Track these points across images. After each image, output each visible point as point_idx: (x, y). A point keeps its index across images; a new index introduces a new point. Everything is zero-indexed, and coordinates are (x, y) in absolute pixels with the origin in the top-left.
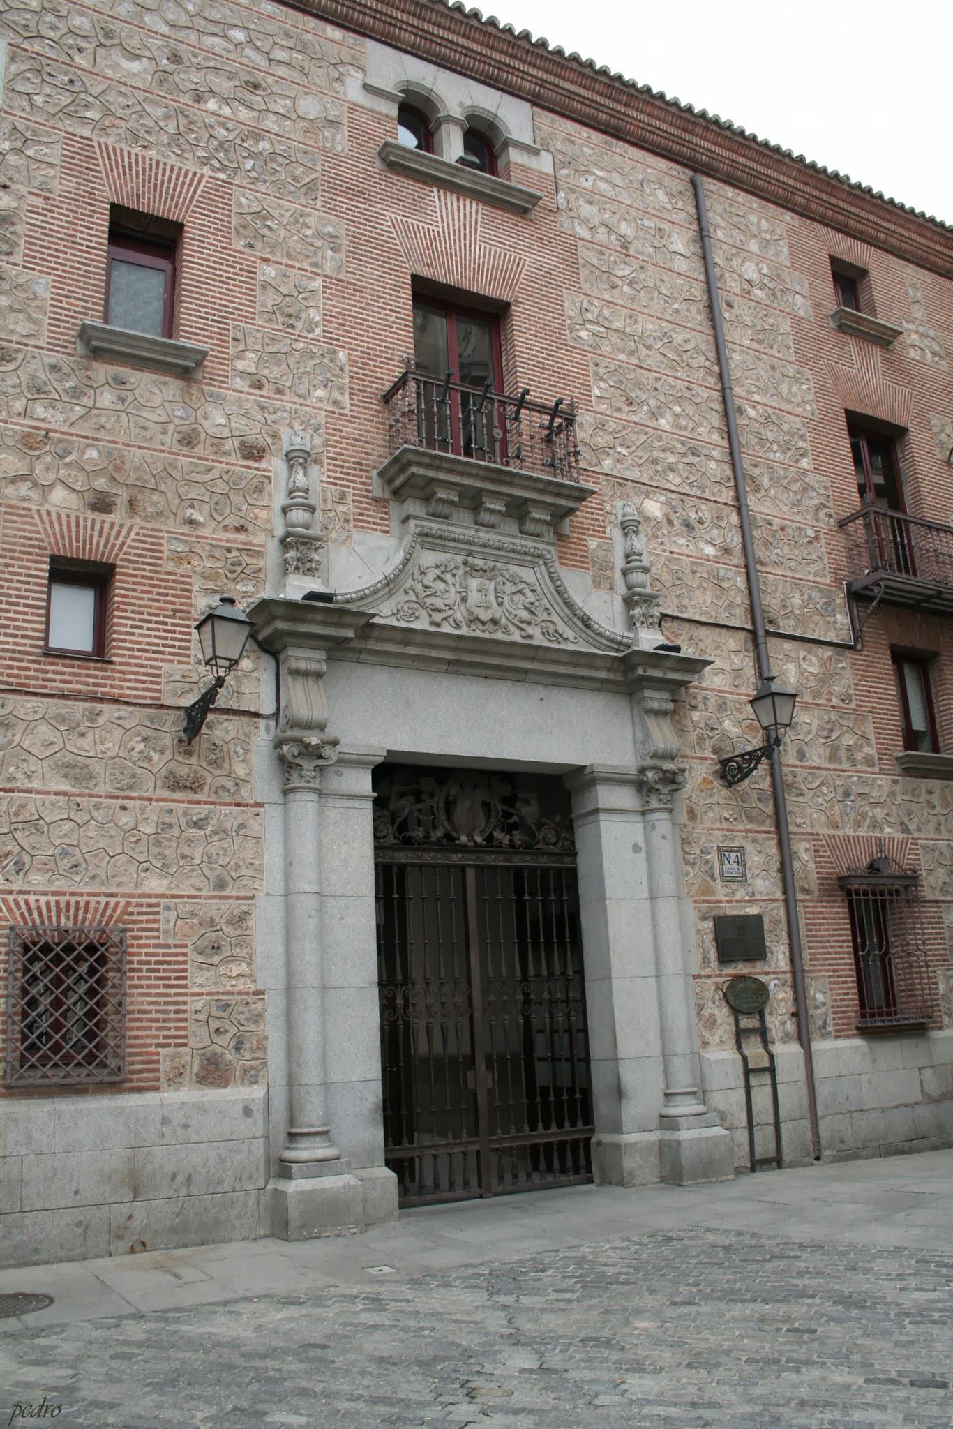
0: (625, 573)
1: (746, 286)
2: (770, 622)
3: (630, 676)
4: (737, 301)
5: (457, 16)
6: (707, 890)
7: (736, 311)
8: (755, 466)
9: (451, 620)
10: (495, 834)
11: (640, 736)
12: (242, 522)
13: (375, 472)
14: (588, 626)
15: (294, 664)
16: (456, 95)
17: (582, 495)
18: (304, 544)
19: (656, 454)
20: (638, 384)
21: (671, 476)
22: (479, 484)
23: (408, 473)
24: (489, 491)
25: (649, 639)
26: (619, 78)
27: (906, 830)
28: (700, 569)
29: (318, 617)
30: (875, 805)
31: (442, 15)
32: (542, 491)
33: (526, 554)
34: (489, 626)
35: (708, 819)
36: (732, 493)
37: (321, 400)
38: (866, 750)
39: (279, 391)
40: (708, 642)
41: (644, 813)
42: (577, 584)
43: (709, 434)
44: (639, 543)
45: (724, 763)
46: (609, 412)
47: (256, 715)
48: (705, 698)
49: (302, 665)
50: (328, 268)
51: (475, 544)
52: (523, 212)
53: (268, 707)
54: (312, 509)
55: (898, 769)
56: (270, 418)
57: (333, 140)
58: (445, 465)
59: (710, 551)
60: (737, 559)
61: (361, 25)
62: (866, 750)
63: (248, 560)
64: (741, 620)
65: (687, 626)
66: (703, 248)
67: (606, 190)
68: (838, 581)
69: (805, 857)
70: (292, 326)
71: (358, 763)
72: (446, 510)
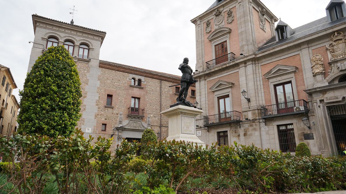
16: (137, 77)
42: (143, 123)
52: (142, 89)
59: (157, 119)
60: (160, 120)
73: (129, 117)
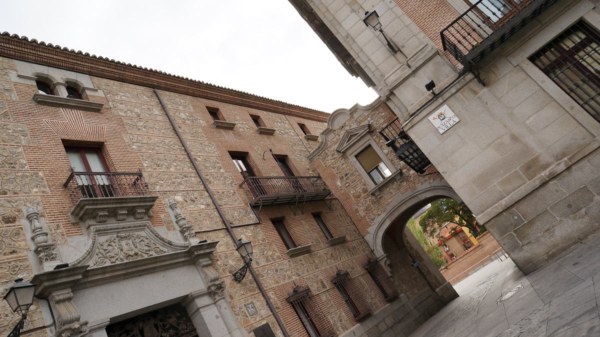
0: (177, 222)
1: (183, 120)
2: (231, 224)
3: (193, 256)
4: (182, 126)
5: (50, 48)
6: (247, 322)
7: (183, 129)
8: (207, 176)
9: (119, 259)
10: (163, 335)
11: (203, 276)
12: (13, 249)
13: (69, 214)
14: (171, 245)
15: (57, 298)
16: (58, 76)
17: (154, 199)
18: (47, 249)
19: (173, 180)
20: (159, 159)
21: (181, 186)
22: (114, 206)
23: (85, 209)
24: (119, 207)
25: (194, 242)
26: (119, 63)
27: (299, 275)
28: (202, 214)
29: (64, 275)
30: (286, 271)
31: (44, 49)
32: (139, 202)
33: (140, 226)
34: (135, 257)
35: (237, 297)
36: (203, 186)
37: (36, 192)
38: (276, 254)
39: (15, 193)
40: (214, 237)
41: (215, 303)
42: (162, 231)
43: (188, 169)
44: (178, 211)
45: (235, 275)
46: (152, 171)
47: (44, 327)
48: (220, 256)
49: (61, 297)
50: (23, 143)
51: (119, 228)
52: (98, 111)
53: (48, 321)
54: (46, 234)
55: (288, 257)
56: (14, 205)
57: (11, 97)
58: (99, 202)
59: (203, 207)
61: (10, 55)
62: (276, 254)
63: (21, 264)
64: (222, 226)
65: (205, 234)
66: (165, 111)
67: (126, 99)
68: (246, 204)
69: (273, 296)
70: (14, 167)
71: (99, 328)
72: (104, 219)
73: (82, 219)
